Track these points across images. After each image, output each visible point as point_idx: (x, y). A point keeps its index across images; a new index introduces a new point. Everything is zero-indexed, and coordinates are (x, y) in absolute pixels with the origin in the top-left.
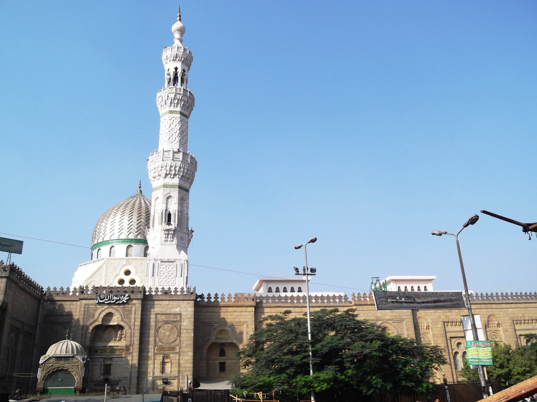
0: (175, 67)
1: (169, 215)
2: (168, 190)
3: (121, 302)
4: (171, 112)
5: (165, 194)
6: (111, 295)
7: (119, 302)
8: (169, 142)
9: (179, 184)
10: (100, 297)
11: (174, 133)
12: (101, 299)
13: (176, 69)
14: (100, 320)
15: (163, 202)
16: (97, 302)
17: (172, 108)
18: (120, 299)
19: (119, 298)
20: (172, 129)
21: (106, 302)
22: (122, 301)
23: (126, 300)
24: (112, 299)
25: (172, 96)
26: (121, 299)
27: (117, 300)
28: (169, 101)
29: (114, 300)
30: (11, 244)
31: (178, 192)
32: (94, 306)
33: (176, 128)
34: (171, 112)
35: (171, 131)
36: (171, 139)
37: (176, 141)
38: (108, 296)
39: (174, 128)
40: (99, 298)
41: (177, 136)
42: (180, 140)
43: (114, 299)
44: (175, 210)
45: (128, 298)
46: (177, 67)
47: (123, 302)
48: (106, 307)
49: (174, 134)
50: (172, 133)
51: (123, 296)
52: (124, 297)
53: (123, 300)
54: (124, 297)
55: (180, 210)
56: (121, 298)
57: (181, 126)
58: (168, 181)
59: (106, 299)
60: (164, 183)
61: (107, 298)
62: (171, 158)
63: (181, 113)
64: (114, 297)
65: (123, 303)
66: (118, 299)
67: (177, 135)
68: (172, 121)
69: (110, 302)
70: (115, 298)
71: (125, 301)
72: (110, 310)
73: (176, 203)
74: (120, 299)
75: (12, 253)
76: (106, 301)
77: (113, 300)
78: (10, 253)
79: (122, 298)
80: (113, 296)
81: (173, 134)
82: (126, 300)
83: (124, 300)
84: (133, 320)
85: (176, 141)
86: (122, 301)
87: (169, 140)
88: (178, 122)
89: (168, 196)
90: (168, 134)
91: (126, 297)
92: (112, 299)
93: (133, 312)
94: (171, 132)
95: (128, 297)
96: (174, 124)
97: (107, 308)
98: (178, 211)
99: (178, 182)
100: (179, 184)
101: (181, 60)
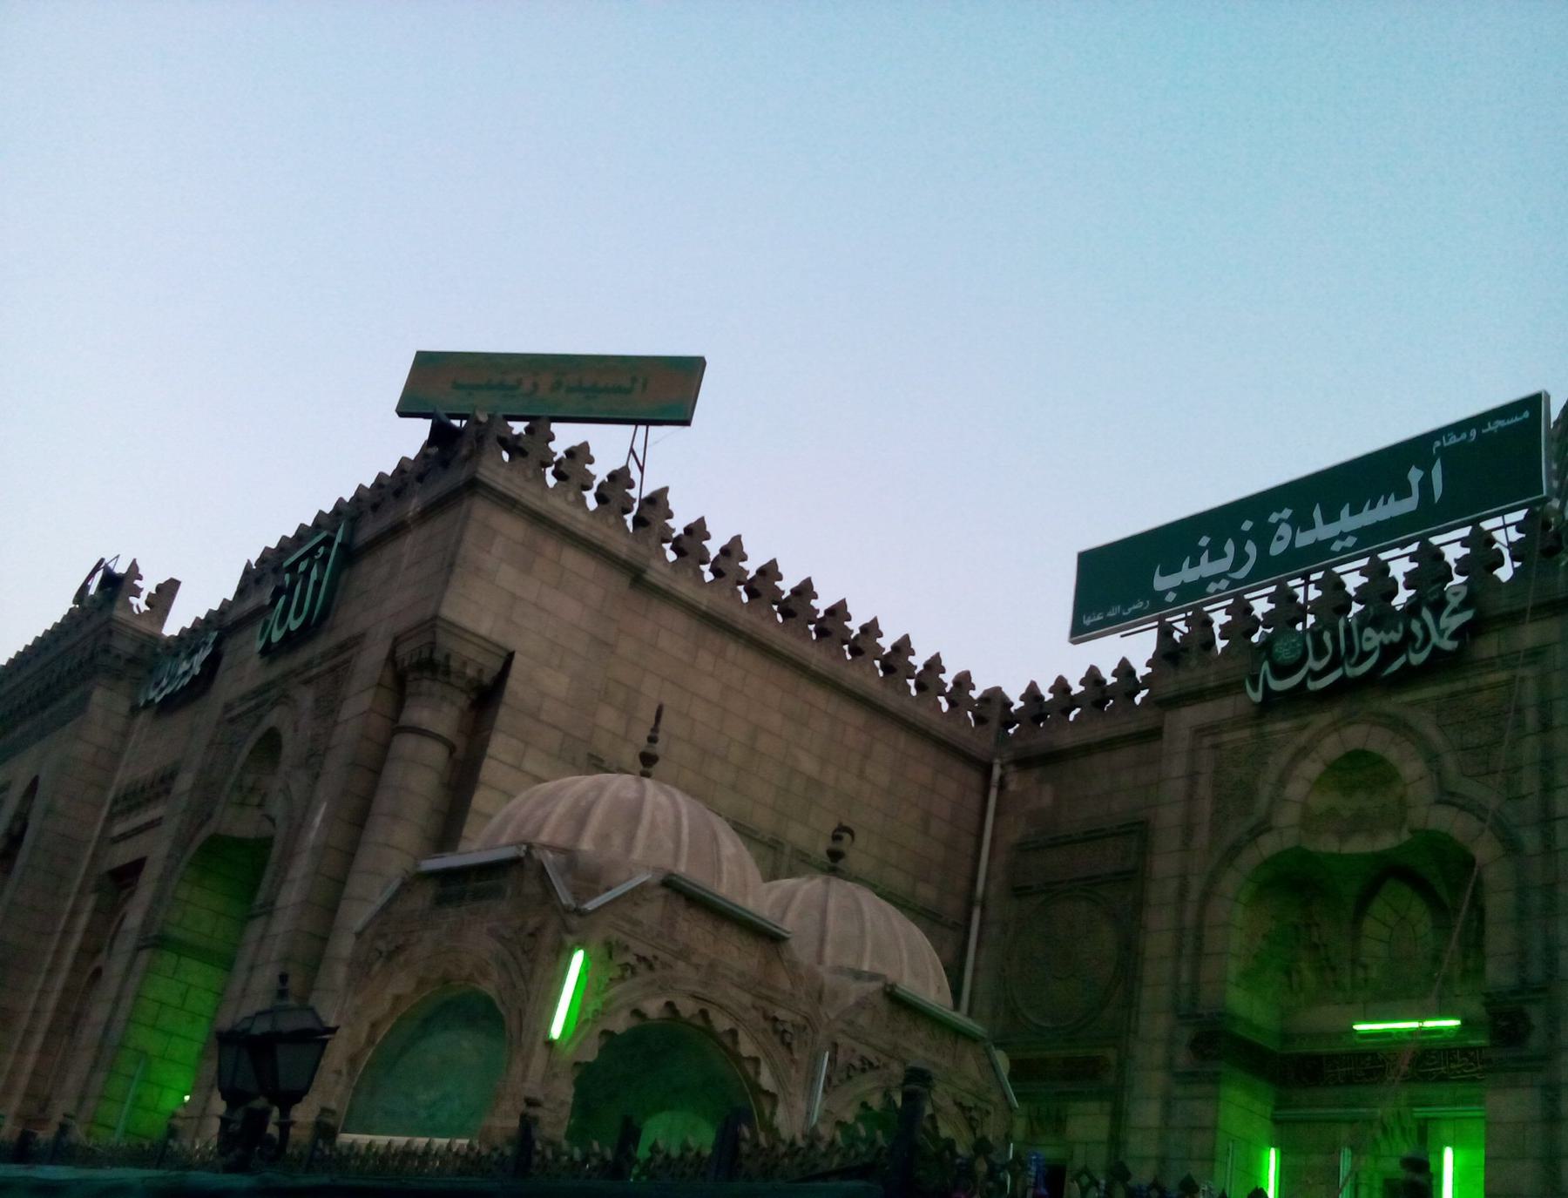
3: (1417, 659)
6: (1342, 623)
7: (1407, 665)
10: (1270, 657)
12: (1281, 671)
14: (1288, 816)
16: (1257, 697)
18: (1409, 636)
19: (1401, 627)
21: (1313, 686)
22: (1429, 648)
23: (1453, 636)
24: (1350, 649)
26: (1420, 634)
27: (1389, 652)
29: (1370, 653)
30: (634, 380)
32: (1246, 733)
38: (1327, 636)
40: (1266, 666)
43: (1367, 647)
45: (1467, 615)
47: (1436, 649)
48: (1321, 720)
51: (1426, 614)
52: (1437, 618)
53: (1435, 639)
54: (1437, 618)
56: (1416, 626)
59: (1313, 664)
61: (1320, 651)
64: (1368, 632)
65: (1440, 664)
66: (1395, 637)
69: (1343, 678)
70: (1373, 639)
71: (1449, 645)
72: (1357, 736)
74: (1409, 636)
75: (652, 428)
76: (1316, 675)
77: (1365, 656)
78: (642, 429)
79: (1425, 628)
80: (1361, 630)
82: (1453, 636)
83: (1441, 633)
84: (1530, 782)
86: (1429, 648)
91: (1446, 613)
92: (1350, 649)
93: (1531, 718)
95: (1465, 605)
97: (1335, 726)
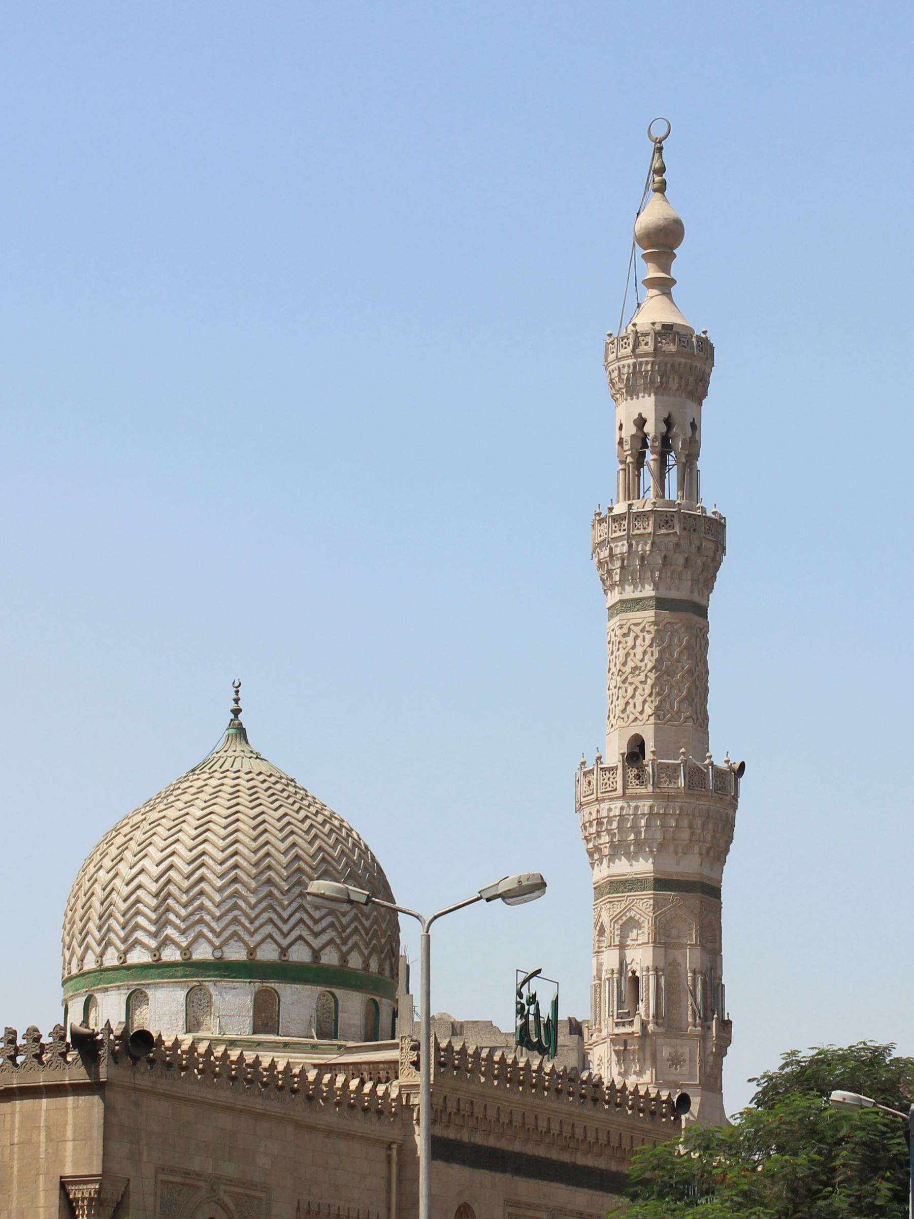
0: (636, 416)
1: (635, 980)
2: (621, 902)
4: (626, 605)
5: (615, 913)
8: (626, 719)
9: (654, 873)
11: (638, 685)
13: (641, 422)
15: (612, 944)
17: (630, 593)
20: (631, 673)
25: (621, 548)
28: (618, 564)
31: (651, 901)
33: (643, 664)
34: (626, 605)
35: (630, 680)
36: (630, 708)
37: (645, 716)
39: (640, 664)
41: (650, 695)
42: (657, 708)
44: (646, 965)
46: (644, 416)
49: (640, 686)
50: (634, 686)
55: (661, 965)
57: (661, 652)
58: (623, 867)
60: (608, 877)
62: (620, 791)
63: (661, 603)
67: (647, 691)
68: (630, 640)
73: (648, 943)
81: (636, 689)
85: (645, 716)
87: (625, 716)
88: (649, 637)
89: (624, 918)
90: (622, 692)
94: (631, 684)
96: (639, 650)
98: (656, 970)
99: (652, 869)
100: (654, 873)
101: (652, 382)
